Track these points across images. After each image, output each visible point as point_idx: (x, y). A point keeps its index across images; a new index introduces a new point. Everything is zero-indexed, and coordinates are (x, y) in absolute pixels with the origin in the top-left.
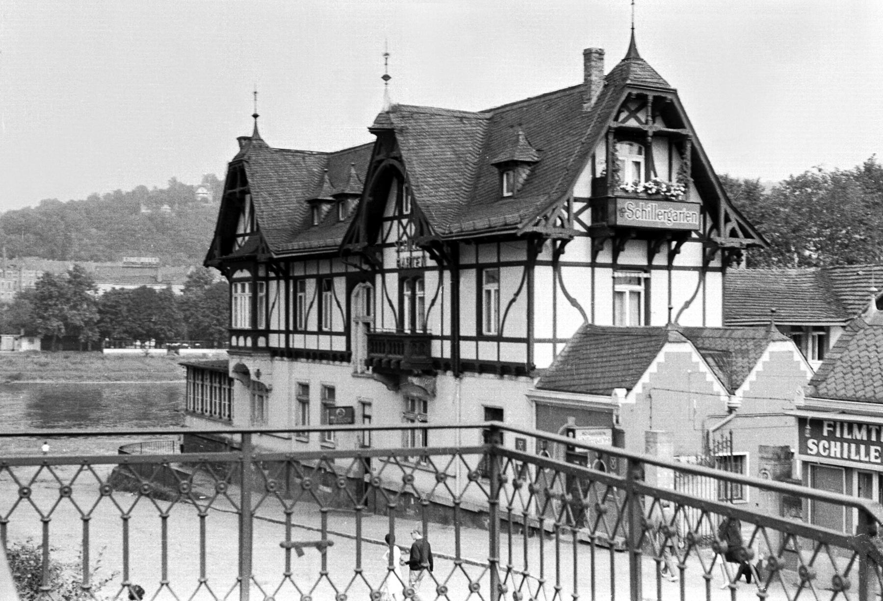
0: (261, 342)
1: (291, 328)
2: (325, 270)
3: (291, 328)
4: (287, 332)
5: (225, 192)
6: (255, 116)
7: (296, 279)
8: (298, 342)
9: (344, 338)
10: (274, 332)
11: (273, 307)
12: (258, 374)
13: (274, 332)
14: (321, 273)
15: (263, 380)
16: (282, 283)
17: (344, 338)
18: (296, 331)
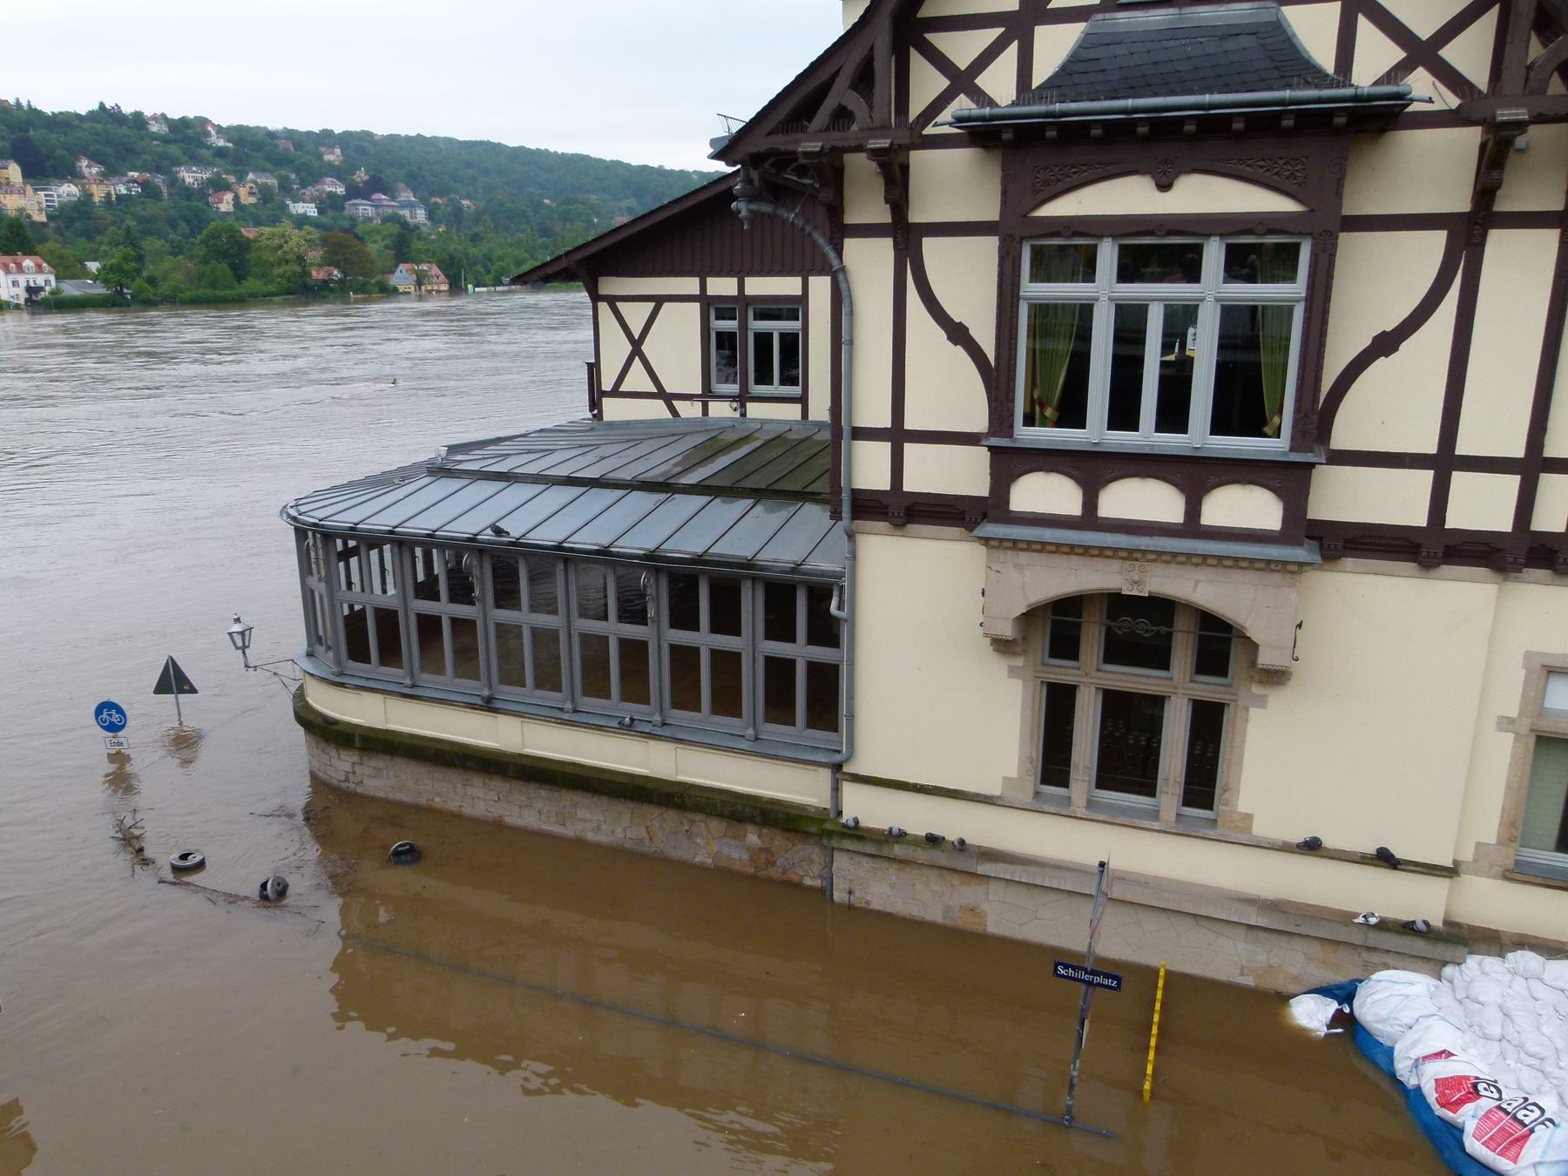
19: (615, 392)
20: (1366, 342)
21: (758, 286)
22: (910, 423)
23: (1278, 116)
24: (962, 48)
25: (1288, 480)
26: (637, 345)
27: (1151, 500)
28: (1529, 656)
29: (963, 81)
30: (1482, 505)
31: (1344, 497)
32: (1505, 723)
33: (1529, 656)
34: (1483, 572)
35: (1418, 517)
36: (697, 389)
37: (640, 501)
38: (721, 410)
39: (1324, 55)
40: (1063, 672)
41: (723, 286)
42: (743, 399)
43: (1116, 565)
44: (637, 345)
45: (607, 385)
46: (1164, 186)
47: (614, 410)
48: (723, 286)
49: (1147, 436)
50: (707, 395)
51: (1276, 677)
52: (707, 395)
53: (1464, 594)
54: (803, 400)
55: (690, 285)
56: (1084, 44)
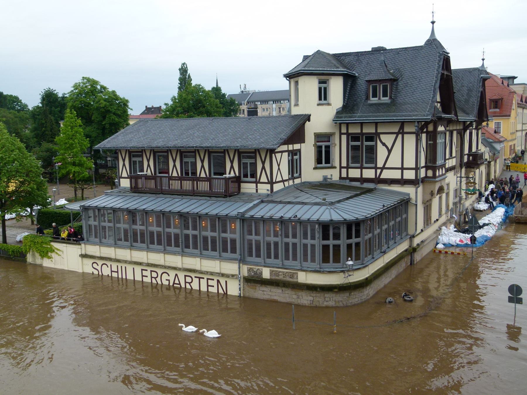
2: (451, 129)
19: (276, 182)
21: (297, 146)
22: (405, 167)
26: (279, 165)
35: (399, 177)
37: (316, 208)
38: (291, 182)
41: (291, 147)
42: (293, 178)
44: (279, 165)
45: (274, 181)
47: (277, 187)
48: (291, 147)
50: (289, 179)
52: (289, 179)
54: (300, 176)
55: (284, 148)
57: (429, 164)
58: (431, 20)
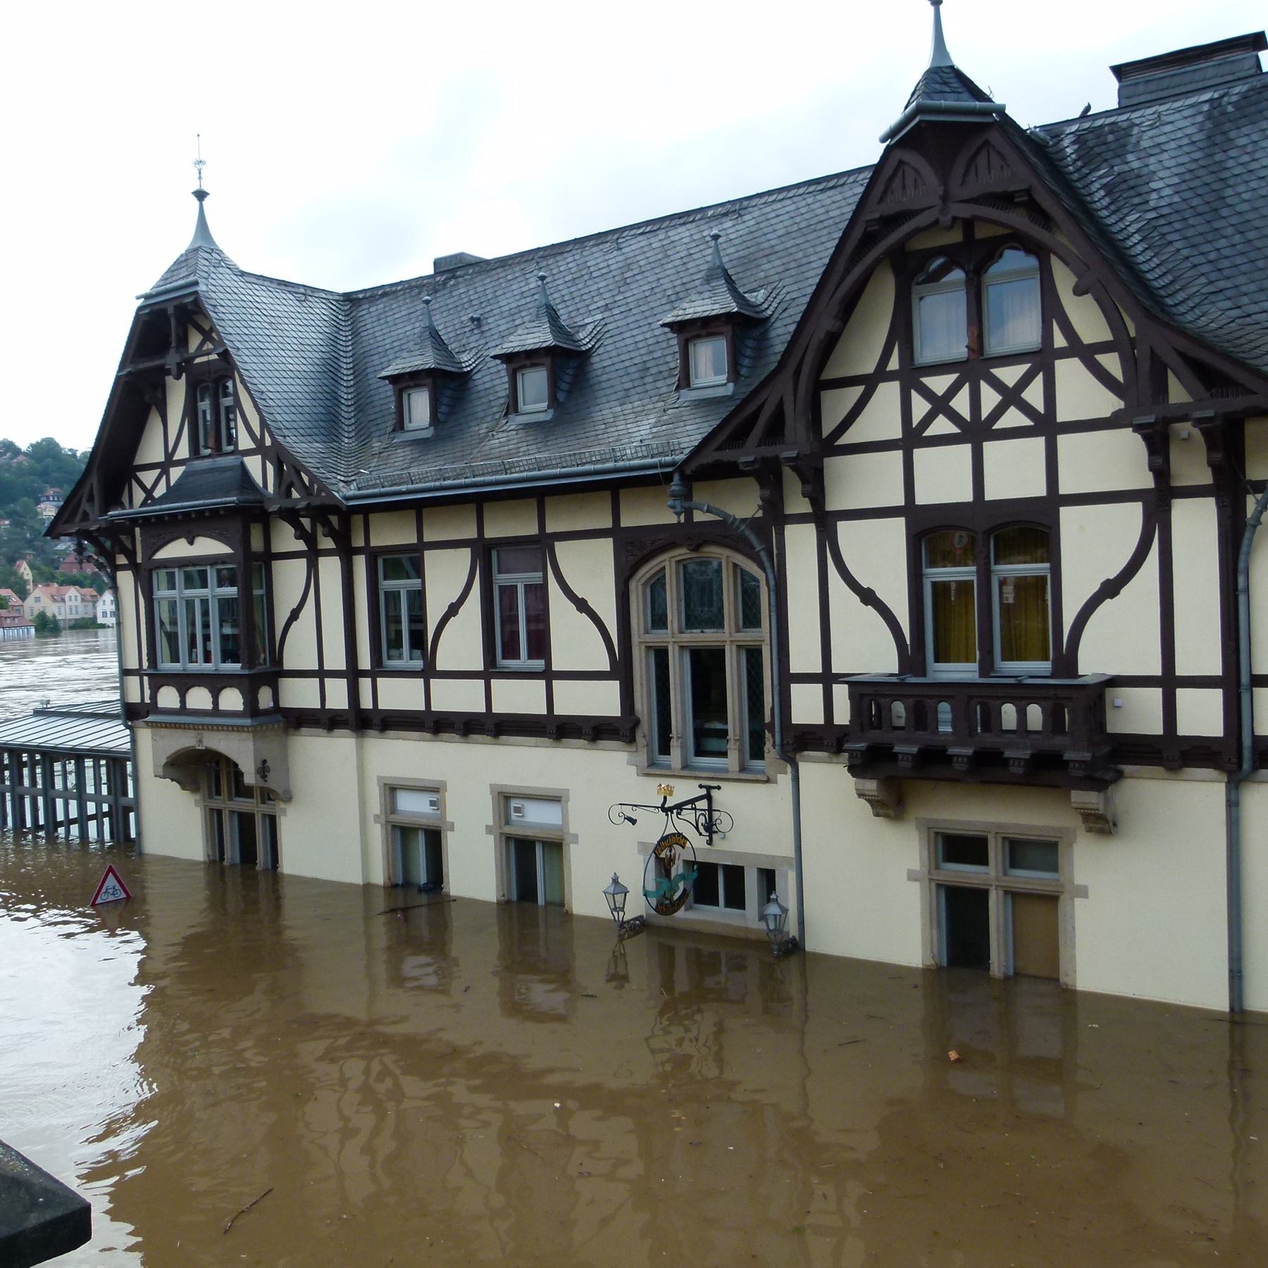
0: (265, 698)
1: (365, 662)
3: (365, 662)
4: (352, 674)
5: (123, 365)
6: (201, 195)
7: (373, 555)
8: (399, 694)
9: (614, 686)
10: (335, 674)
11: (295, 615)
12: (263, 770)
13: (335, 674)
14: (489, 534)
15: (273, 783)
16: (330, 568)
17: (614, 686)
18: (378, 670)
20: (288, 615)
23: (202, 512)
24: (148, 477)
25: (250, 689)
27: (199, 698)
28: (379, 778)
29: (149, 493)
30: (337, 696)
31: (300, 695)
32: (376, 816)
33: (379, 778)
34: (347, 732)
36: (479, 666)
39: (258, 479)
40: (218, 803)
43: (192, 733)
46: (191, 543)
49: (200, 666)
51: (288, 798)
53: (342, 744)
56: (185, 476)
57: (167, 666)
58: (196, 188)
